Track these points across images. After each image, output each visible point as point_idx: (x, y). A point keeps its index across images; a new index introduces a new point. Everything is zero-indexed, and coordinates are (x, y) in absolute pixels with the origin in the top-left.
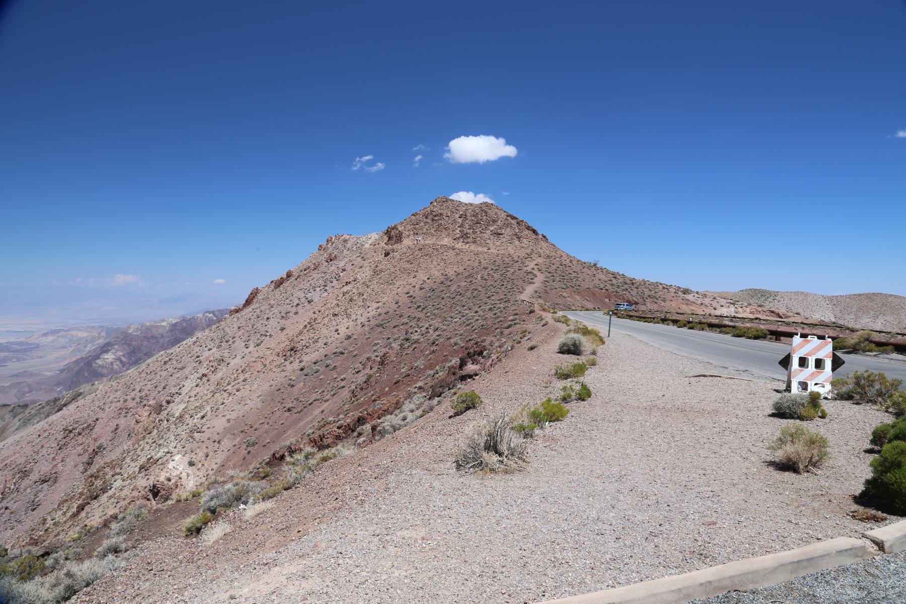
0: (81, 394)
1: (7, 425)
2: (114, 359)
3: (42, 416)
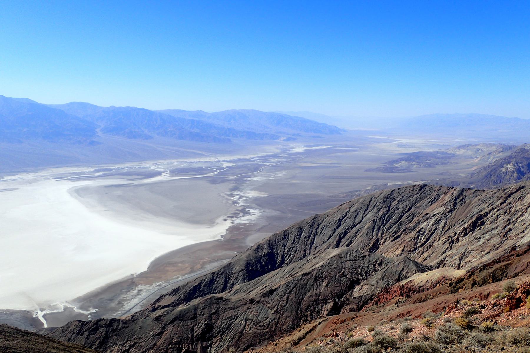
3: (494, 199)
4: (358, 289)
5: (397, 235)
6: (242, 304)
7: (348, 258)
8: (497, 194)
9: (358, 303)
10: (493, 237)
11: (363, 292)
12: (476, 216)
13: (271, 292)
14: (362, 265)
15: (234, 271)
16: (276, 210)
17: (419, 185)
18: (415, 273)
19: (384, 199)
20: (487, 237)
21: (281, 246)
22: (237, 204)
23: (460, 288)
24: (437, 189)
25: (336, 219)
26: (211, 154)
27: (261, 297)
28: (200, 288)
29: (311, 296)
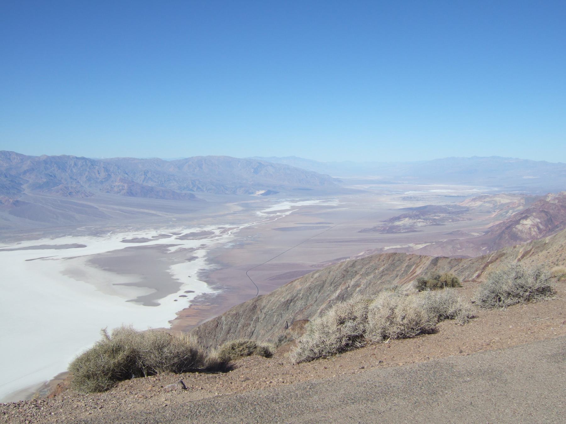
0: (504, 254)
2: (532, 225)
17: (386, 254)
24: (408, 258)
26: (167, 215)
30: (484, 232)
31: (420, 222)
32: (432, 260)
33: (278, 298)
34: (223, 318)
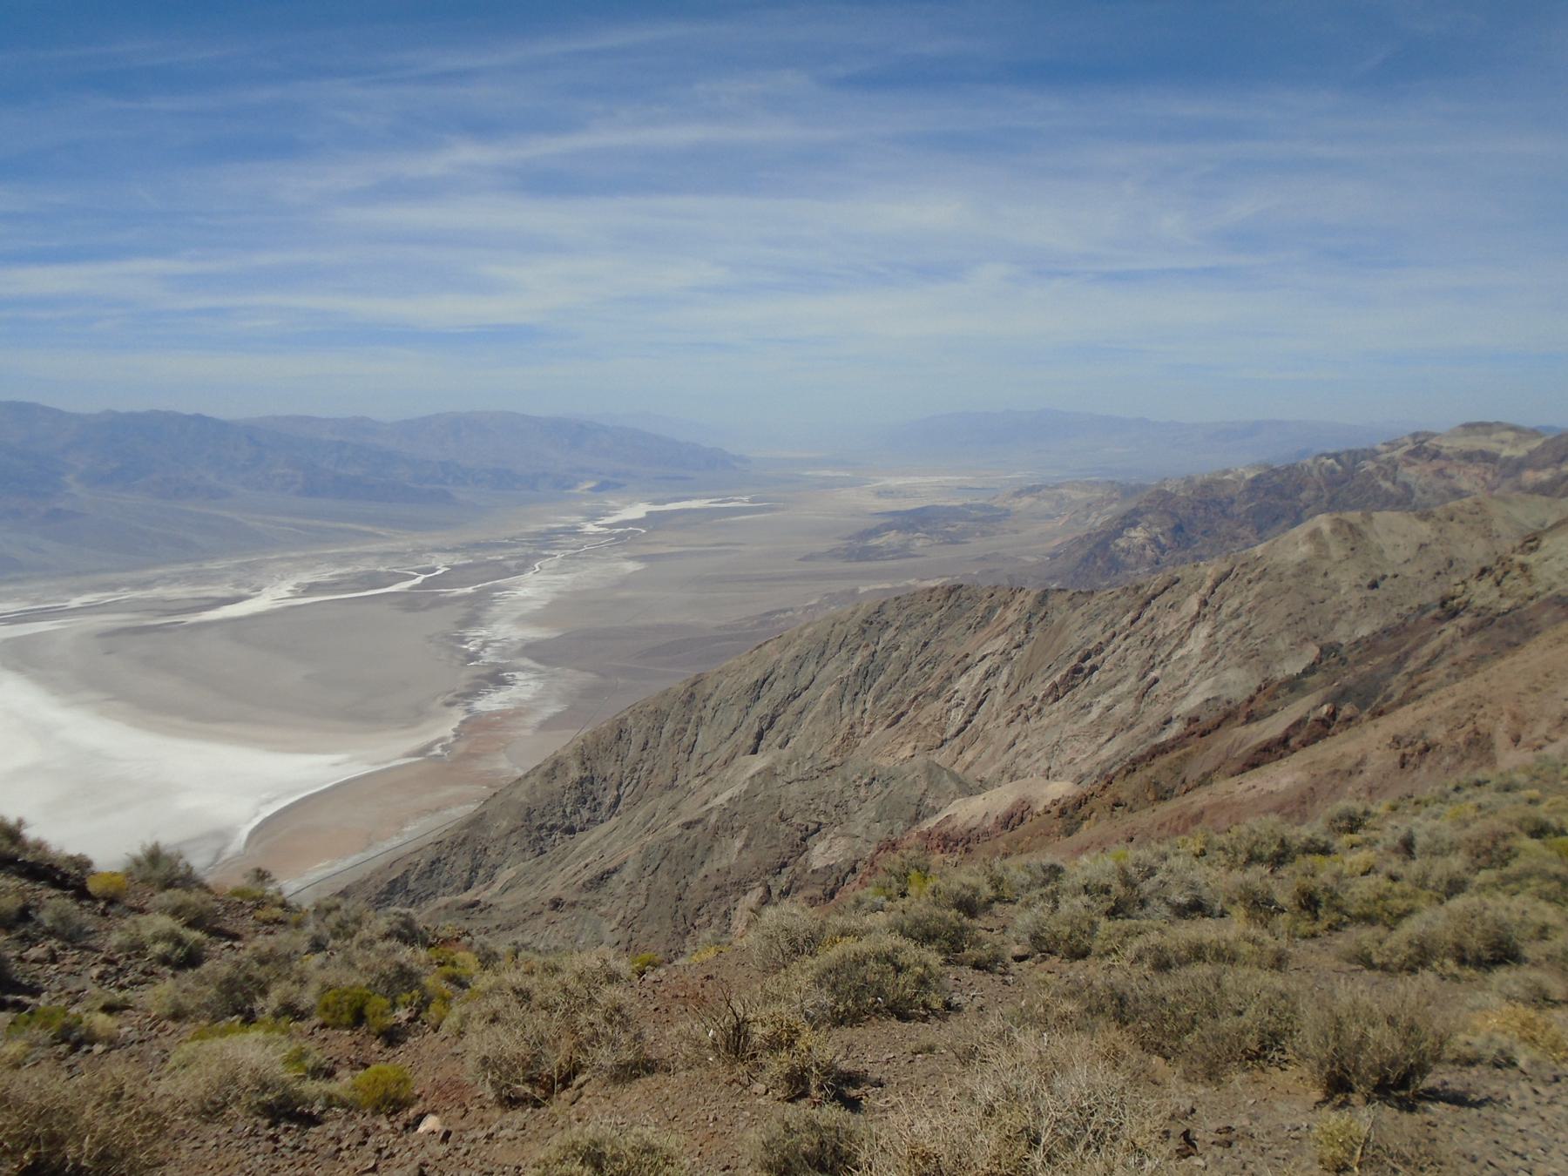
1: (1065, 620)
2: (1146, 538)
3: (1117, 610)
4: (822, 850)
5: (899, 712)
6: (531, 912)
7: (793, 775)
8: (1123, 599)
9: (824, 883)
10: (1119, 702)
11: (835, 855)
12: (1079, 653)
13: (604, 877)
14: (829, 789)
15: (493, 834)
16: (584, 671)
18: (954, 799)
19: (865, 626)
20: (1105, 700)
21: (614, 757)
22: (478, 660)
23: (1084, 818)
24: (986, 595)
25: (748, 681)
27: (580, 891)
28: (406, 883)
29: (706, 876)
30: (1047, 555)
31: (918, 538)
32: (1037, 596)
33: (736, 677)
34: (630, 721)
